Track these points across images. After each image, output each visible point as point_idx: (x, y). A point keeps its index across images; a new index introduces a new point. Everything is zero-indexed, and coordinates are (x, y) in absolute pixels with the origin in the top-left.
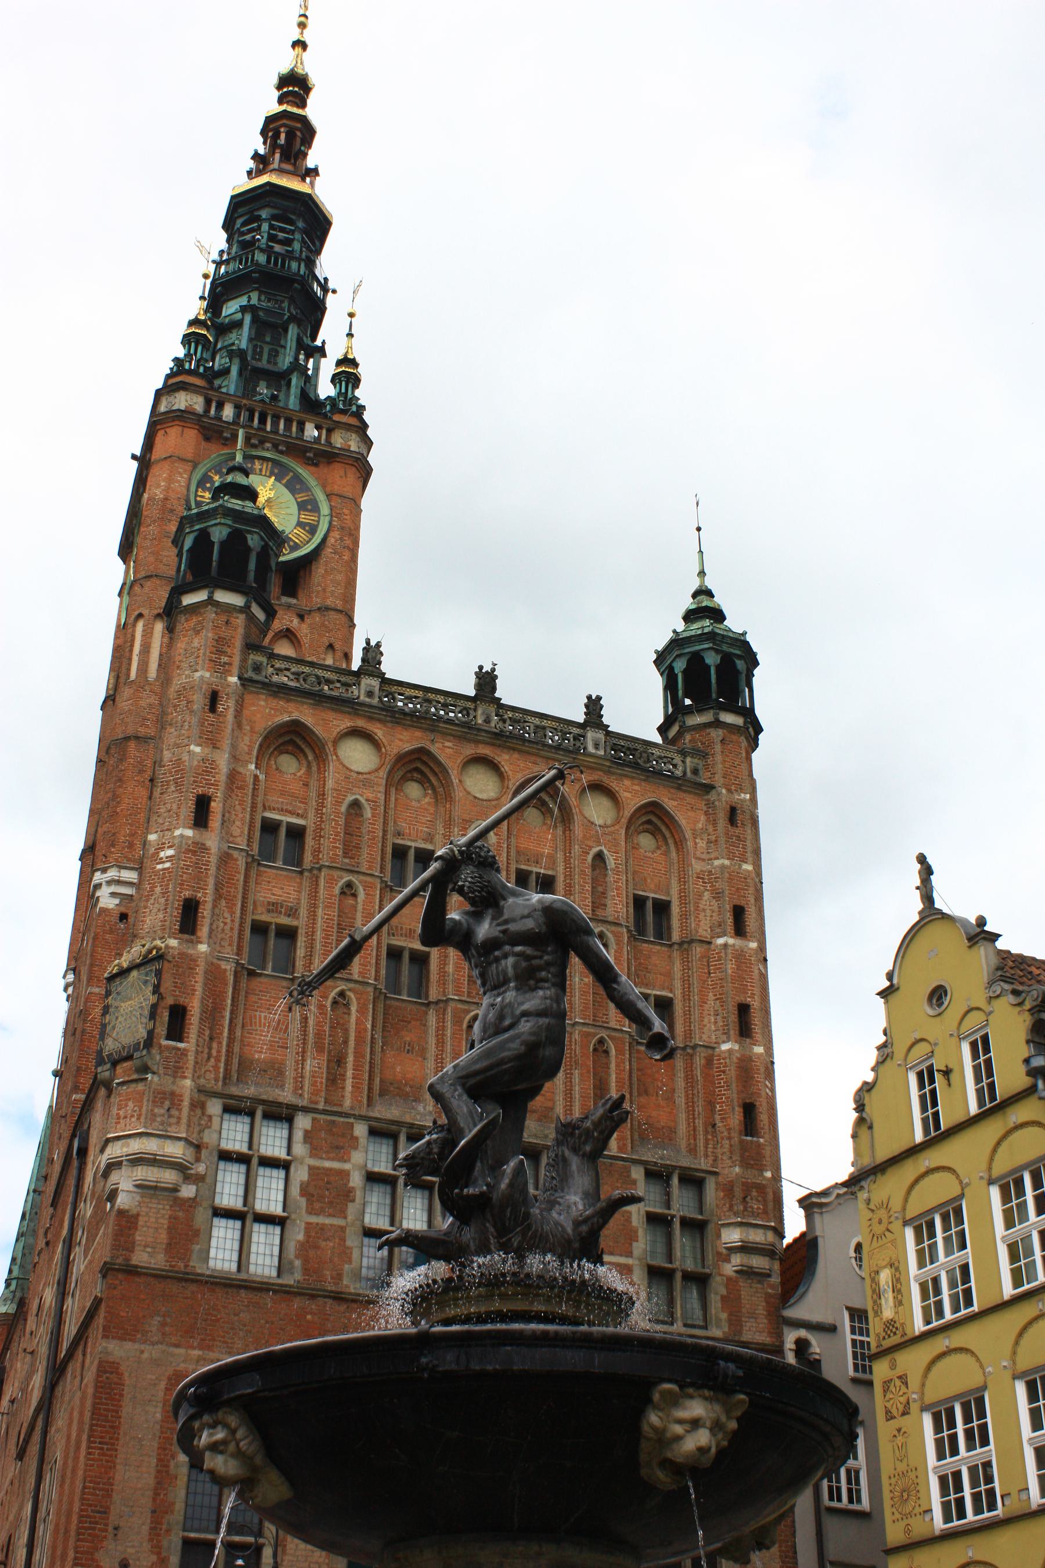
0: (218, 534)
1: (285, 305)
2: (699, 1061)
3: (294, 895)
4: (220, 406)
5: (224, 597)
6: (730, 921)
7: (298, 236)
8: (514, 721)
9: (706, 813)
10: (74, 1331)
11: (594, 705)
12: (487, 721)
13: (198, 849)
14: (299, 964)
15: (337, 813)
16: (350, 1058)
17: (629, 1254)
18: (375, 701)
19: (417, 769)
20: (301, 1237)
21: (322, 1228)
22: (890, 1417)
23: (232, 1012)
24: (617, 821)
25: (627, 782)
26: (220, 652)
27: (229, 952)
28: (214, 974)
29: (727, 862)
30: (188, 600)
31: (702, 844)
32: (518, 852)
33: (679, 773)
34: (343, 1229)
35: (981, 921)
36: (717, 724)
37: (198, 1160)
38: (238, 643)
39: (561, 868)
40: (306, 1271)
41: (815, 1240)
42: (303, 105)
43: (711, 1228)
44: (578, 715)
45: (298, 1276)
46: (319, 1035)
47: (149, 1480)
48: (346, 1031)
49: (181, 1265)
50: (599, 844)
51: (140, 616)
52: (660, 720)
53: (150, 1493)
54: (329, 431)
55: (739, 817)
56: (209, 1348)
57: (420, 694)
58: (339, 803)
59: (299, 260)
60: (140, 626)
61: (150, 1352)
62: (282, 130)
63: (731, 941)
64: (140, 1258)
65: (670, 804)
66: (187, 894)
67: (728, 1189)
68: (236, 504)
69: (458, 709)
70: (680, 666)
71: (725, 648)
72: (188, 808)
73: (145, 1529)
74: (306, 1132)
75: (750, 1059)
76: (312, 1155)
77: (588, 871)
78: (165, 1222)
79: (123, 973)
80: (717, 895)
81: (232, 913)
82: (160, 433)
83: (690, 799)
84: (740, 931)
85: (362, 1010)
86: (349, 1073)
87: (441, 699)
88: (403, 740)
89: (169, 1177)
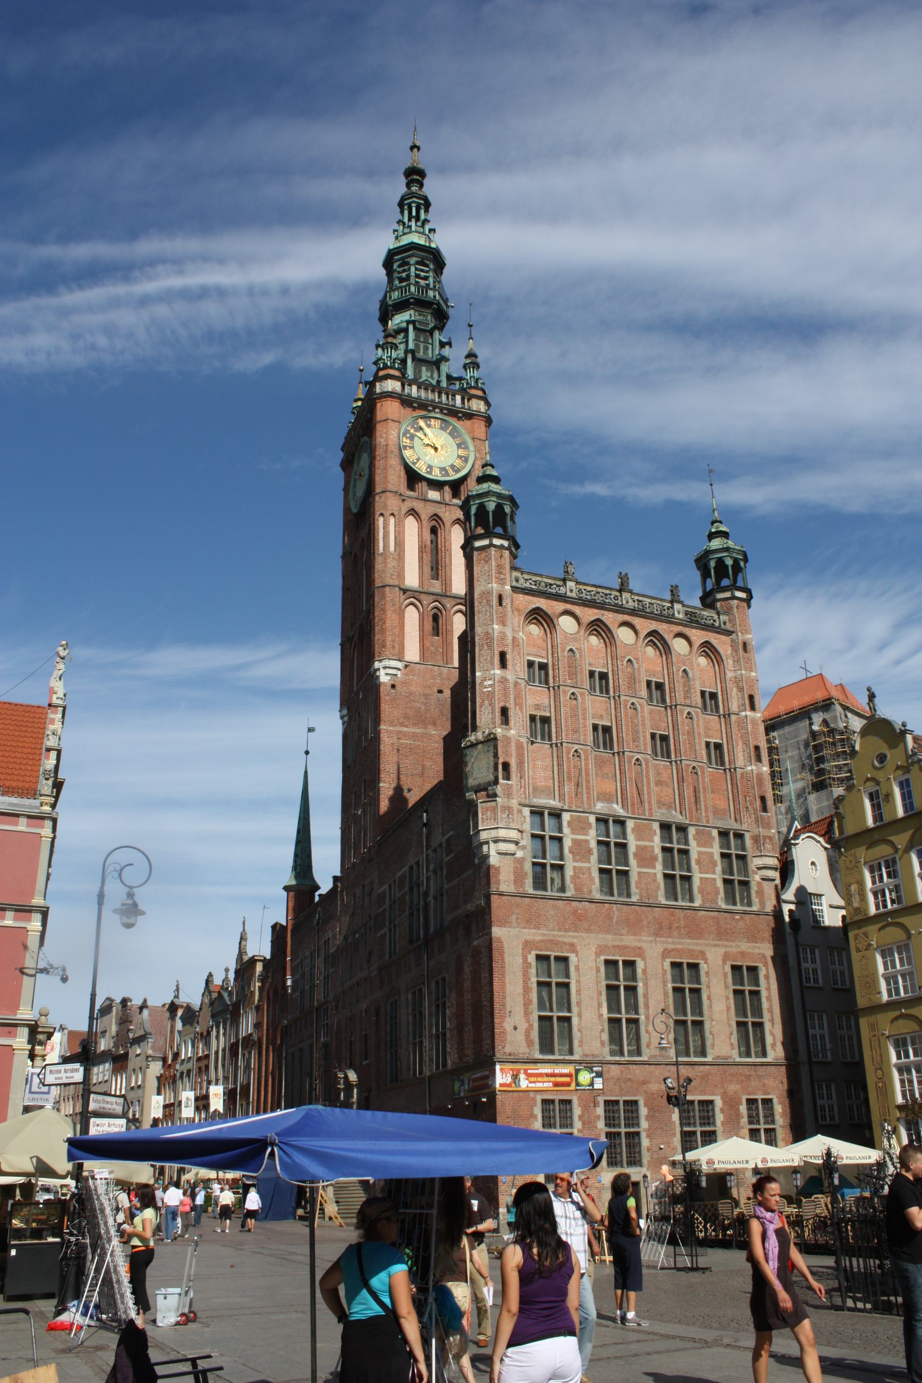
0: (491, 506)
1: (429, 318)
2: (739, 776)
3: (546, 701)
4: (410, 385)
5: (497, 542)
7: (431, 274)
9: (732, 646)
10: (448, 918)
11: (674, 590)
12: (627, 602)
13: (504, 680)
14: (554, 735)
15: (563, 657)
16: (584, 783)
17: (714, 873)
18: (574, 595)
19: (595, 630)
20: (571, 873)
21: (581, 868)
22: (858, 950)
24: (691, 651)
25: (694, 631)
26: (501, 573)
27: (523, 733)
28: (519, 746)
30: (478, 544)
31: (731, 662)
32: (646, 671)
33: (717, 624)
34: (589, 868)
35: (904, 725)
36: (734, 598)
37: (522, 838)
38: (508, 567)
39: (666, 679)
40: (576, 889)
41: (793, 861)
42: (421, 185)
43: (749, 858)
45: (573, 892)
46: (568, 772)
47: (520, 989)
48: (580, 770)
49: (521, 890)
50: (684, 664)
51: (382, 514)
52: (701, 594)
53: (522, 997)
54: (468, 400)
55: (748, 648)
56: (539, 929)
57: (594, 589)
58: (563, 651)
59: (434, 289)
60: (381, 519)
61: (514, 931)
62: (413, 205)
63: (748, 713)
64: (503, 888)
65: (714, 642)
66: (502, 704)
67: (756, 839)
68: (494, 487)
69: (612, 596)
70: (712, 564)
71: (734, 555)
72: (497, 658)
73: (522, 1012)
74: (569, 822)
75: (762, 774)
76: (572, 833)
77: (682, 681)
79: (473, 745)
80: (741, 689)
82: (379, 405)
83: (723, 637)
85: (586, 759)
86: (585, 791)
87: (604, 591)
88: (589, 615)
89: (511, 847)
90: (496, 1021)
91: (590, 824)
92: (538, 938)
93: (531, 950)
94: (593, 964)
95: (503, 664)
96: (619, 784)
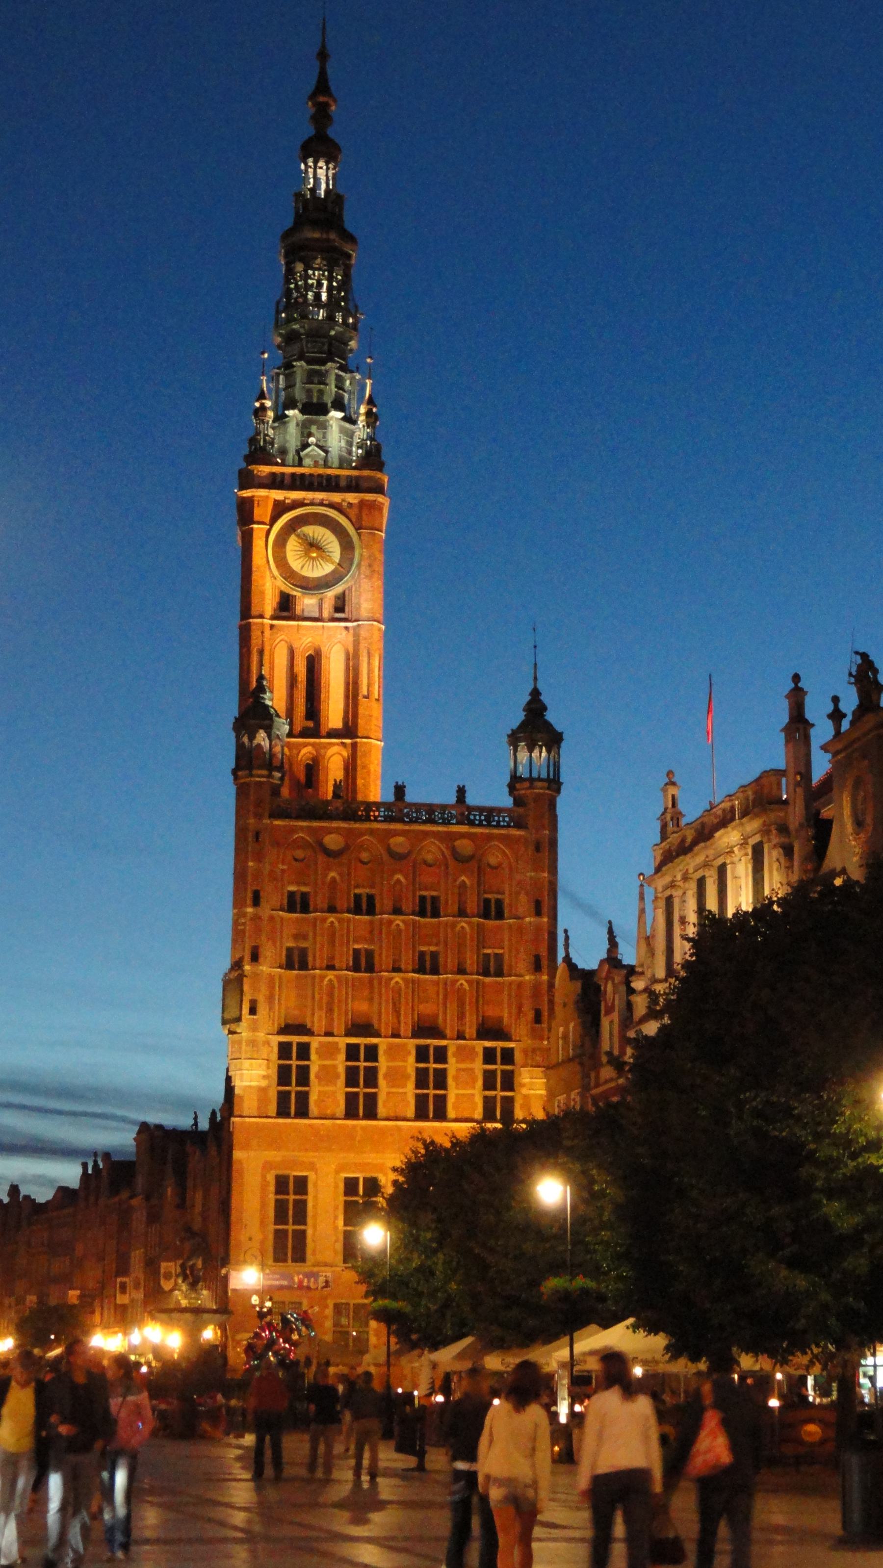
6: (533, 910)
8: (416, 812)
11: (461, 792)
13: (256, 918)
15: (323, 883)
17: (474, 1088)
23: (279, 995)
29: (533, 874)
34: (334, 1093)
44: (452, 799)
61: (252, 1154)
63: (532, 919)
72: (250, 895)
78: (255, 1098)
80: (527, 894)
81: (275, 947)
84: (538, 913)
90: (233, 1234)
91: (338, 1050)
92: (278, 1159)
93: (271, 1169)
94: (331, 1180)
95: (256, 901)
96: (376, 1006)
